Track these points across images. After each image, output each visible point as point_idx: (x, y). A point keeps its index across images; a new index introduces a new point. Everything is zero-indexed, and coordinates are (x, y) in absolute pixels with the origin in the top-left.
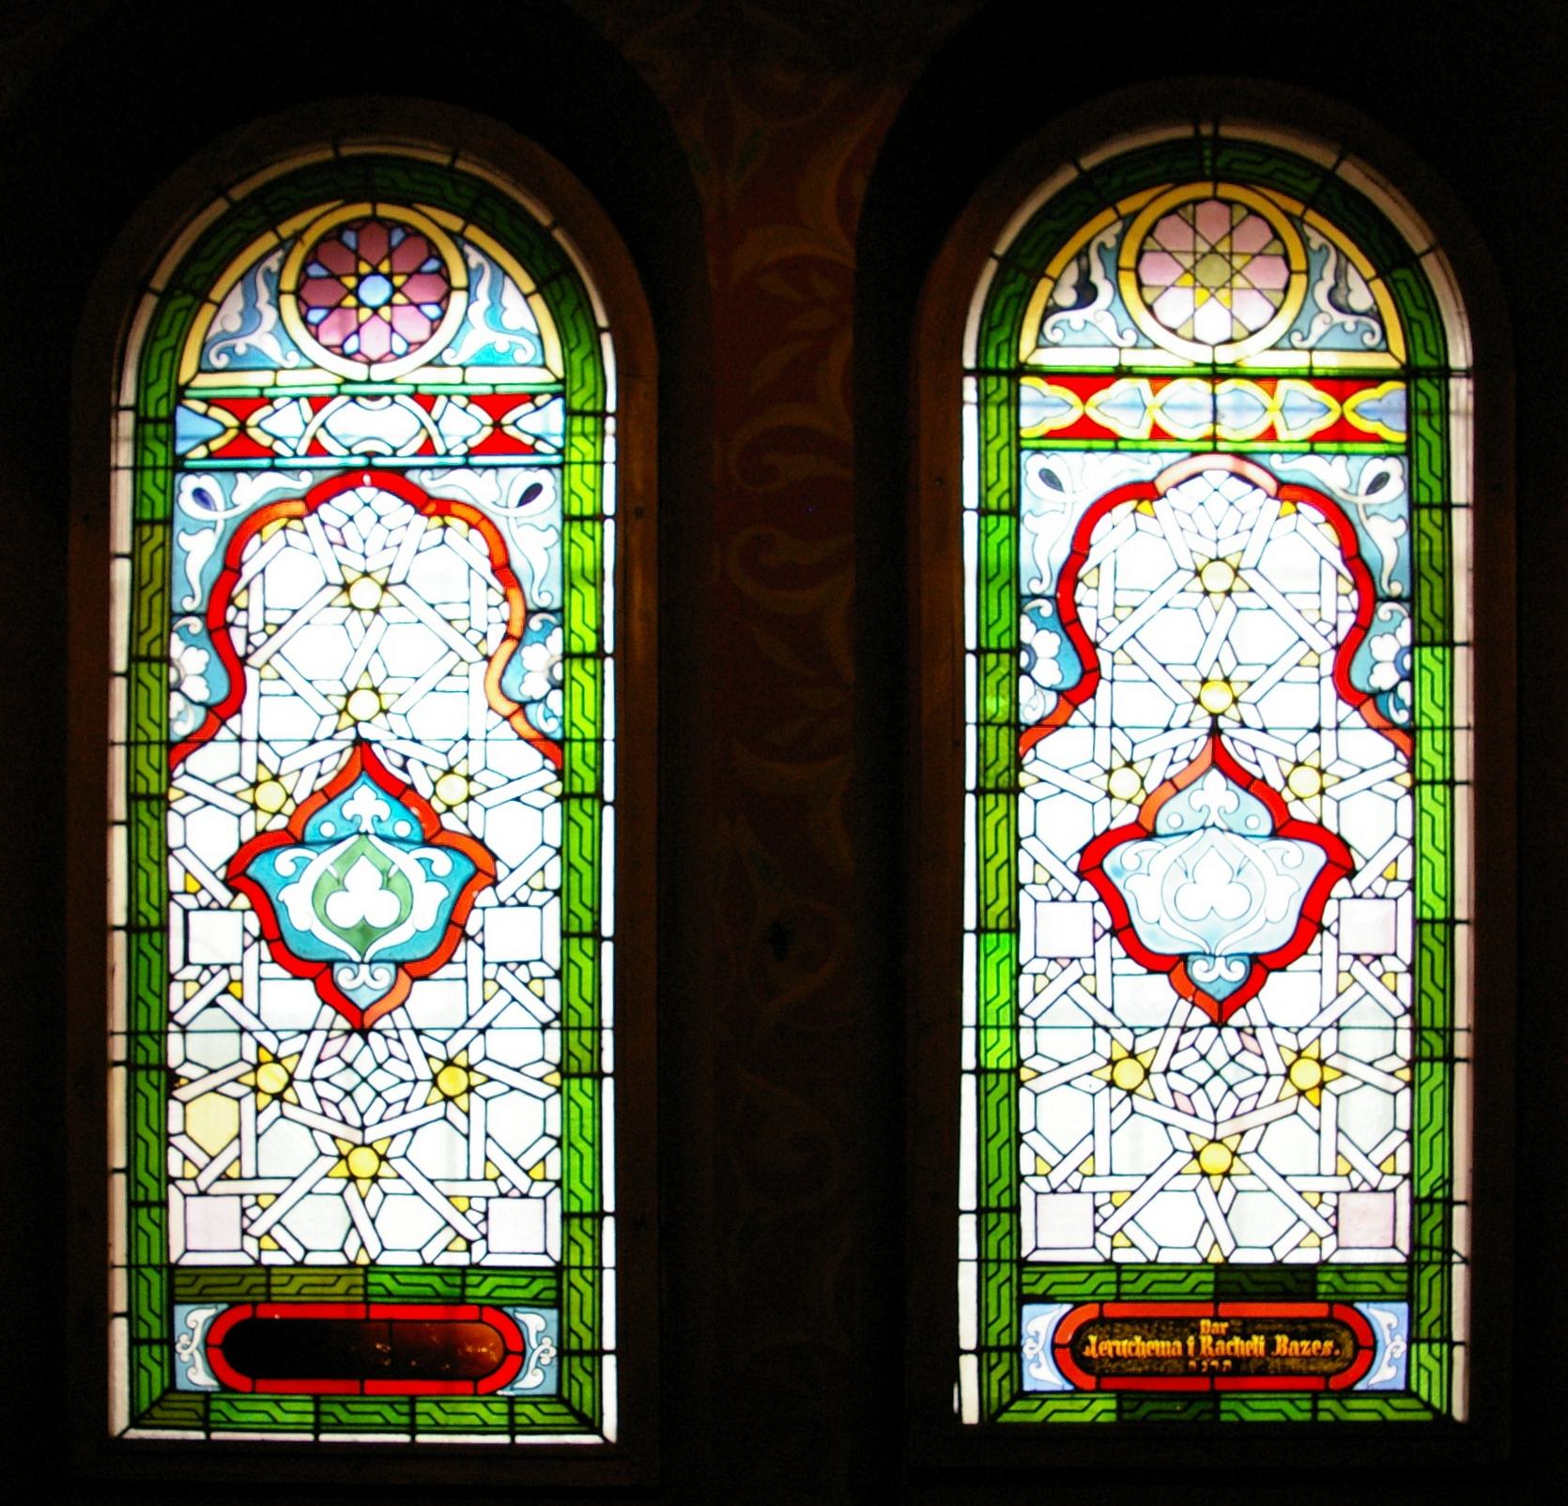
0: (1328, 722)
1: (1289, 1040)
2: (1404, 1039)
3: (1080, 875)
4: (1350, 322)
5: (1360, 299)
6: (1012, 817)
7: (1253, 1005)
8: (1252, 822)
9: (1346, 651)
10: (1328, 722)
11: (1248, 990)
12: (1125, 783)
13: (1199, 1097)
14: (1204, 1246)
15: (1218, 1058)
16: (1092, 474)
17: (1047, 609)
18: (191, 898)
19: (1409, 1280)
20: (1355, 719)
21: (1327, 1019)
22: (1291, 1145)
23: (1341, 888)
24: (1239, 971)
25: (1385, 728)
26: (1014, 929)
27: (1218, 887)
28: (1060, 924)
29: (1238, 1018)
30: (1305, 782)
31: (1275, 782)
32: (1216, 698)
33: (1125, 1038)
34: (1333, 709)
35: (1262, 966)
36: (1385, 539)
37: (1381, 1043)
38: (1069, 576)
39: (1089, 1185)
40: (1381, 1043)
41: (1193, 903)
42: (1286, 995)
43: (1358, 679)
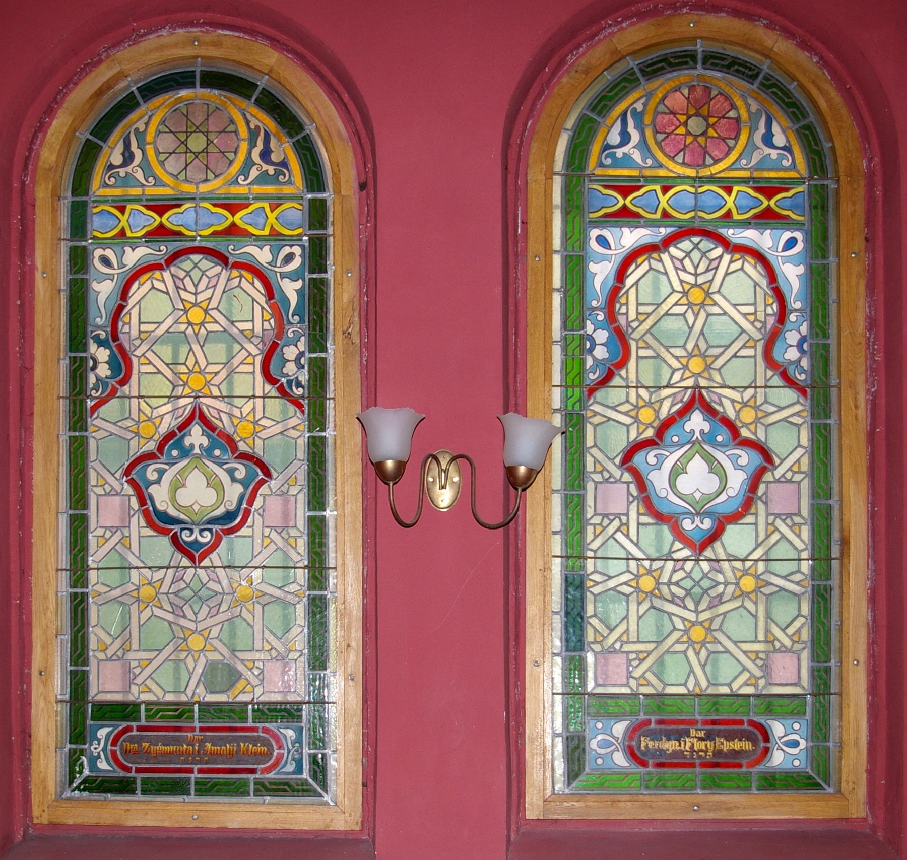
0: (760, 382)
4: (774, 154)
5: (779, 139)
7: (717, 544)
8: (719, 439)
9: (772, 339)
10: (760, 382)
11: (715, 536)
12: (646, 415)
14: (691, 685)
16: (630, 238)
17: (601, 317)
18: (101, 489)
23: (768, 477)
29: (708, 553)
30: (748, 415)
31: (731, 414)
33: (647, 564)
36: (792, 274)
38: (614, 294)
39: (626, 648)
42: (737, 539)
43: (777, 355)
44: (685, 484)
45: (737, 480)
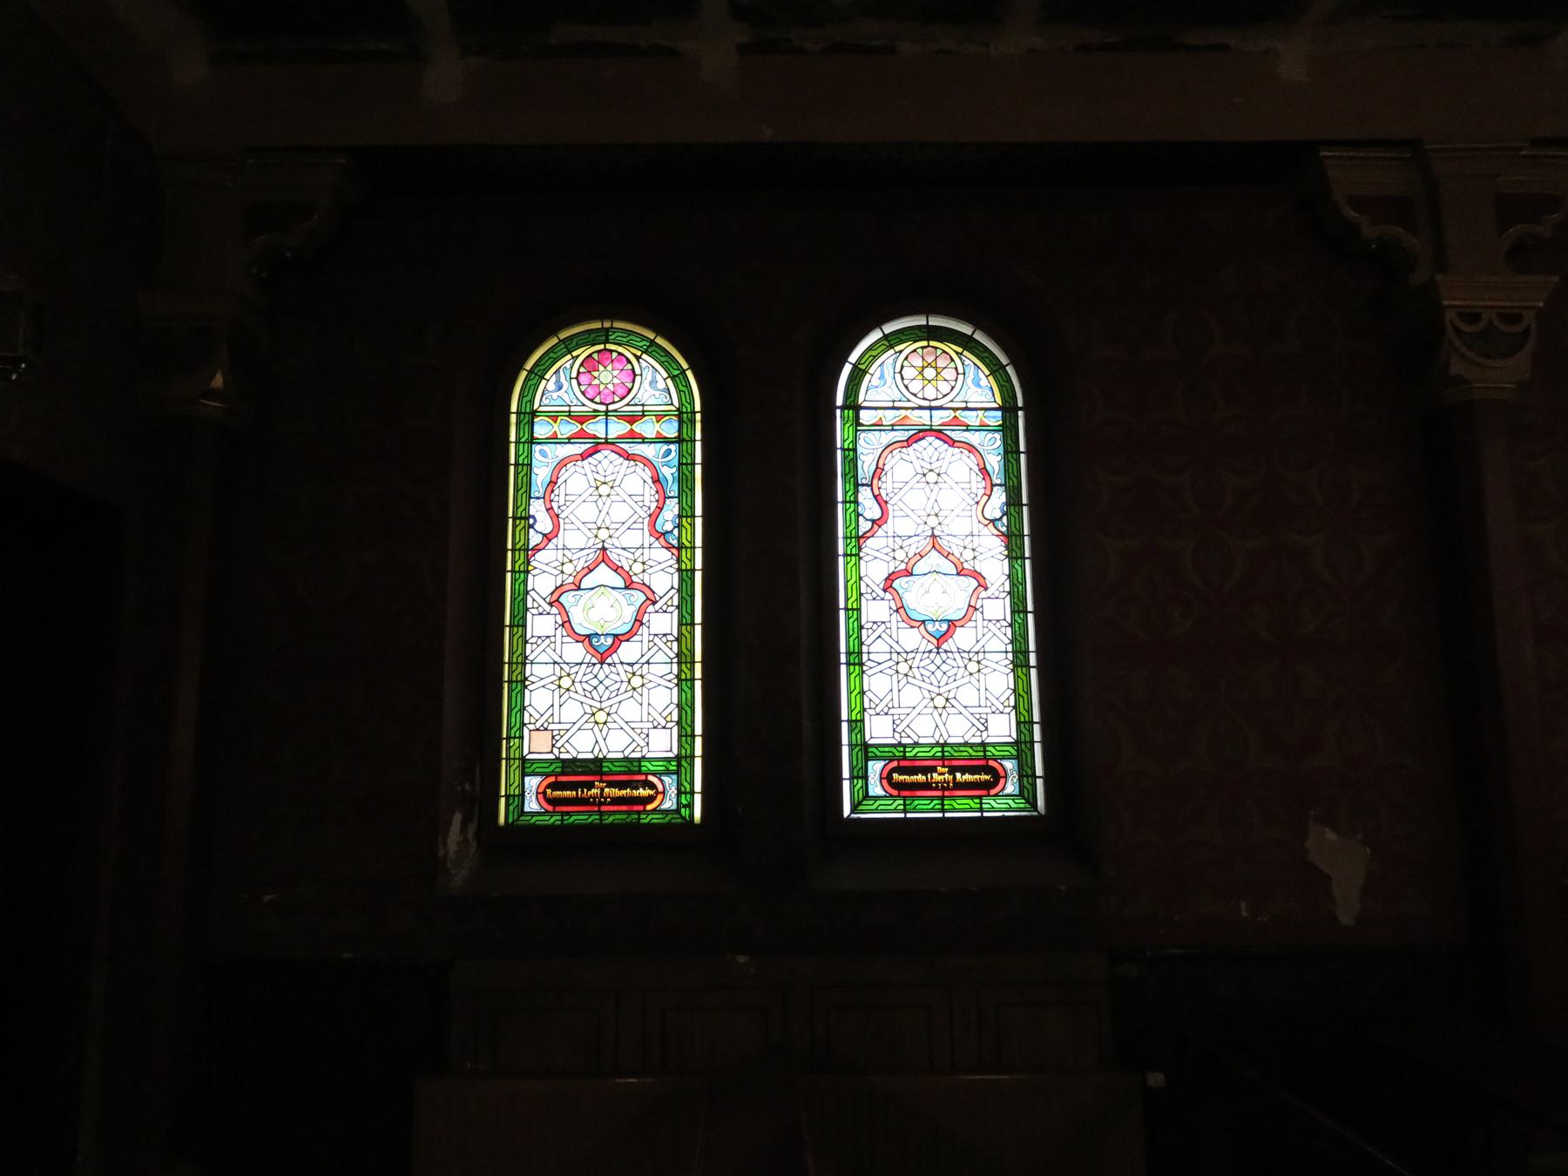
1: (629, 668)
2: (675, 666)
3: (551, 604)
6: (525, 582)
9: (654, 517)
11: (613, 649)
12: (568, 568)
13: (594, 693)
15: (601, 676)
19: (681, 762)
20: (657, 544)
21: (644, 660)
22: (630, 710)
24: (610, 640)
25: (669, 547)
26: (525, 626)
27: (602, 609)
28: (540, 625)
30: (637, 568)
32: (603, 534)
34: (648, 540)
35: (618, 639)
36: (669, 473)
37: (665, 669)
40: (665, 669)
41: (595, 615)
42: (628, 651)
44: (595, 615)
45: (629, 614)
